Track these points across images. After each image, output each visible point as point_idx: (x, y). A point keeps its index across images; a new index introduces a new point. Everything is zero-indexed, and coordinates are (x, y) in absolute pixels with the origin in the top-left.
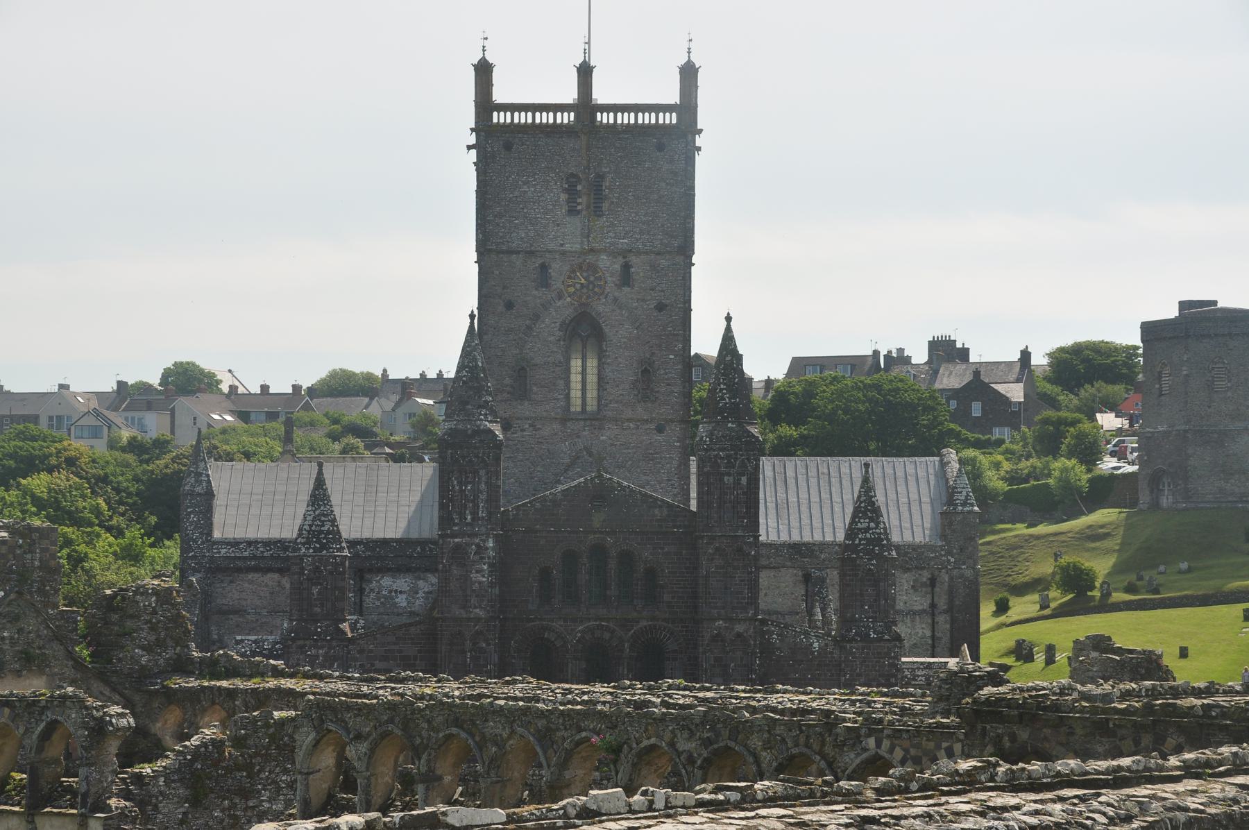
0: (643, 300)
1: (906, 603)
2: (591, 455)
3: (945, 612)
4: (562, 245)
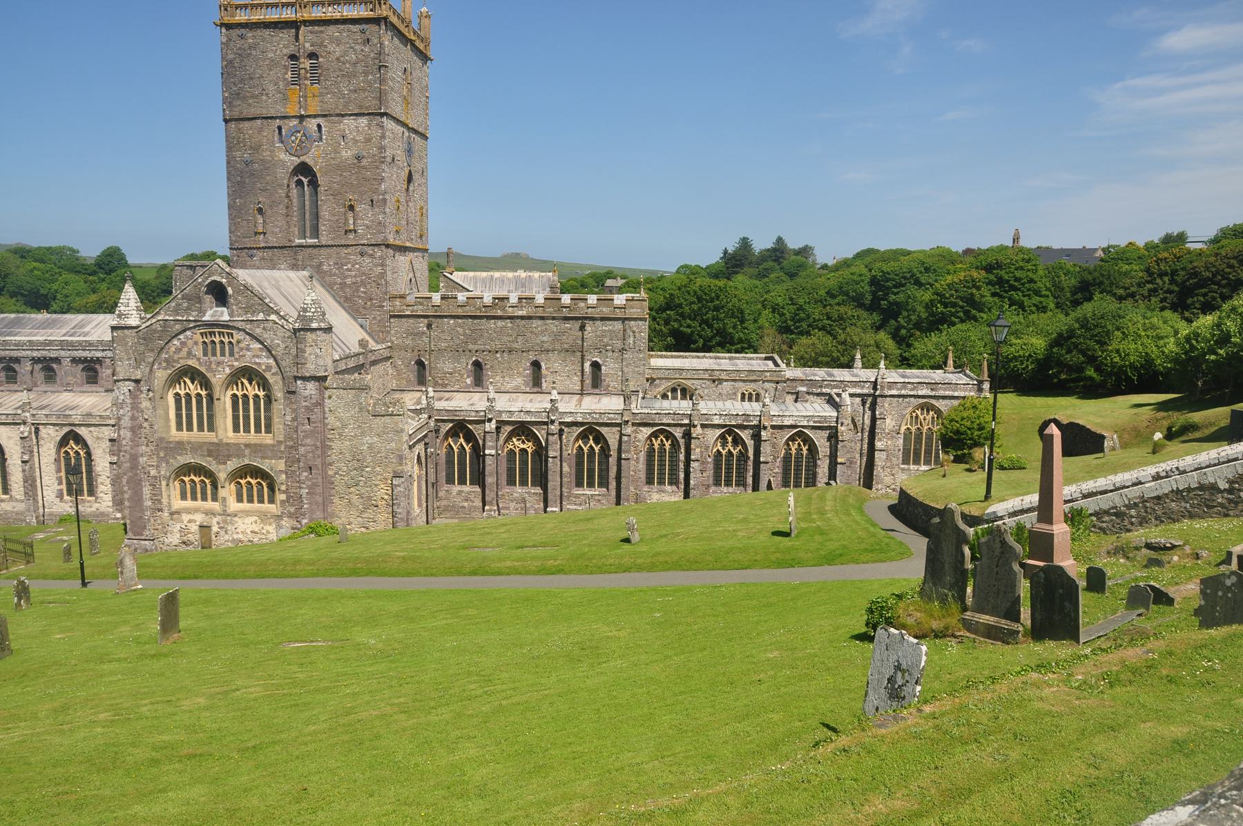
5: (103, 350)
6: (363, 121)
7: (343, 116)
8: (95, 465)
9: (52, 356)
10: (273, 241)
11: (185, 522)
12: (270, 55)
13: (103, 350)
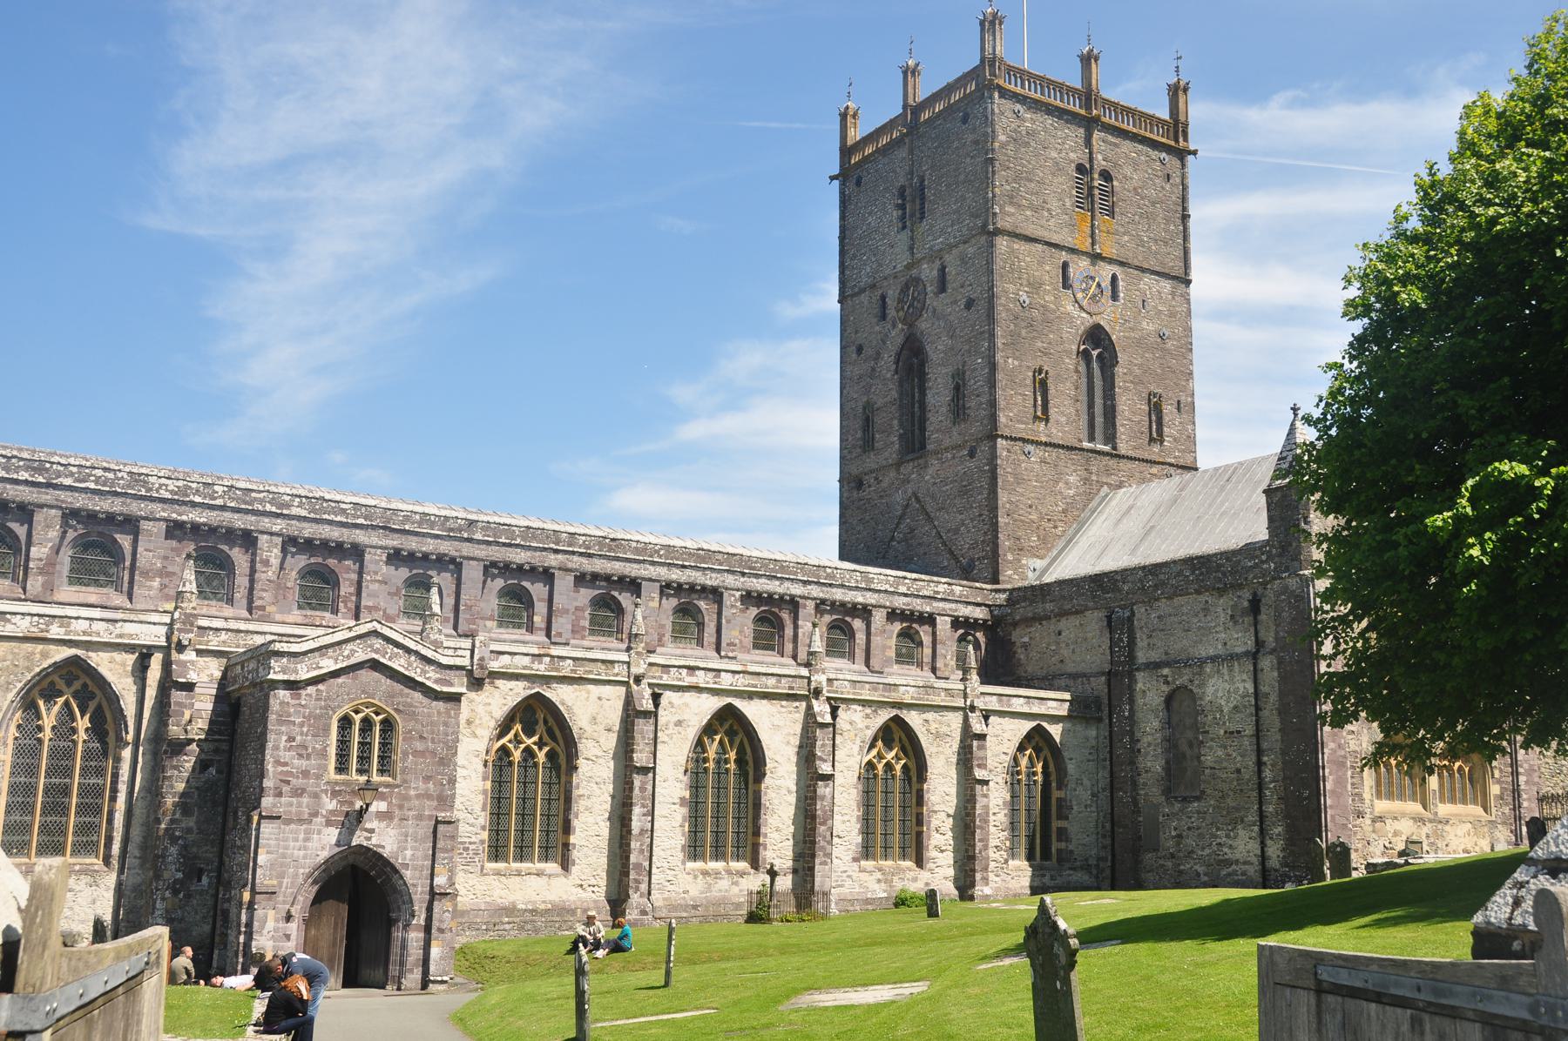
0: (955, 302)
1: (1225, 644)
2: (917, 499)
3: (1273, 651)
4: (895, 267)
5: (805, 583)
6: (1166, 286)
7: (1143, 270)
8: (928, 792)
9: (709, 583)
10: (1058, 436)
11: (1390, 835)
12: (1054, 154)
13: (805, 583)
